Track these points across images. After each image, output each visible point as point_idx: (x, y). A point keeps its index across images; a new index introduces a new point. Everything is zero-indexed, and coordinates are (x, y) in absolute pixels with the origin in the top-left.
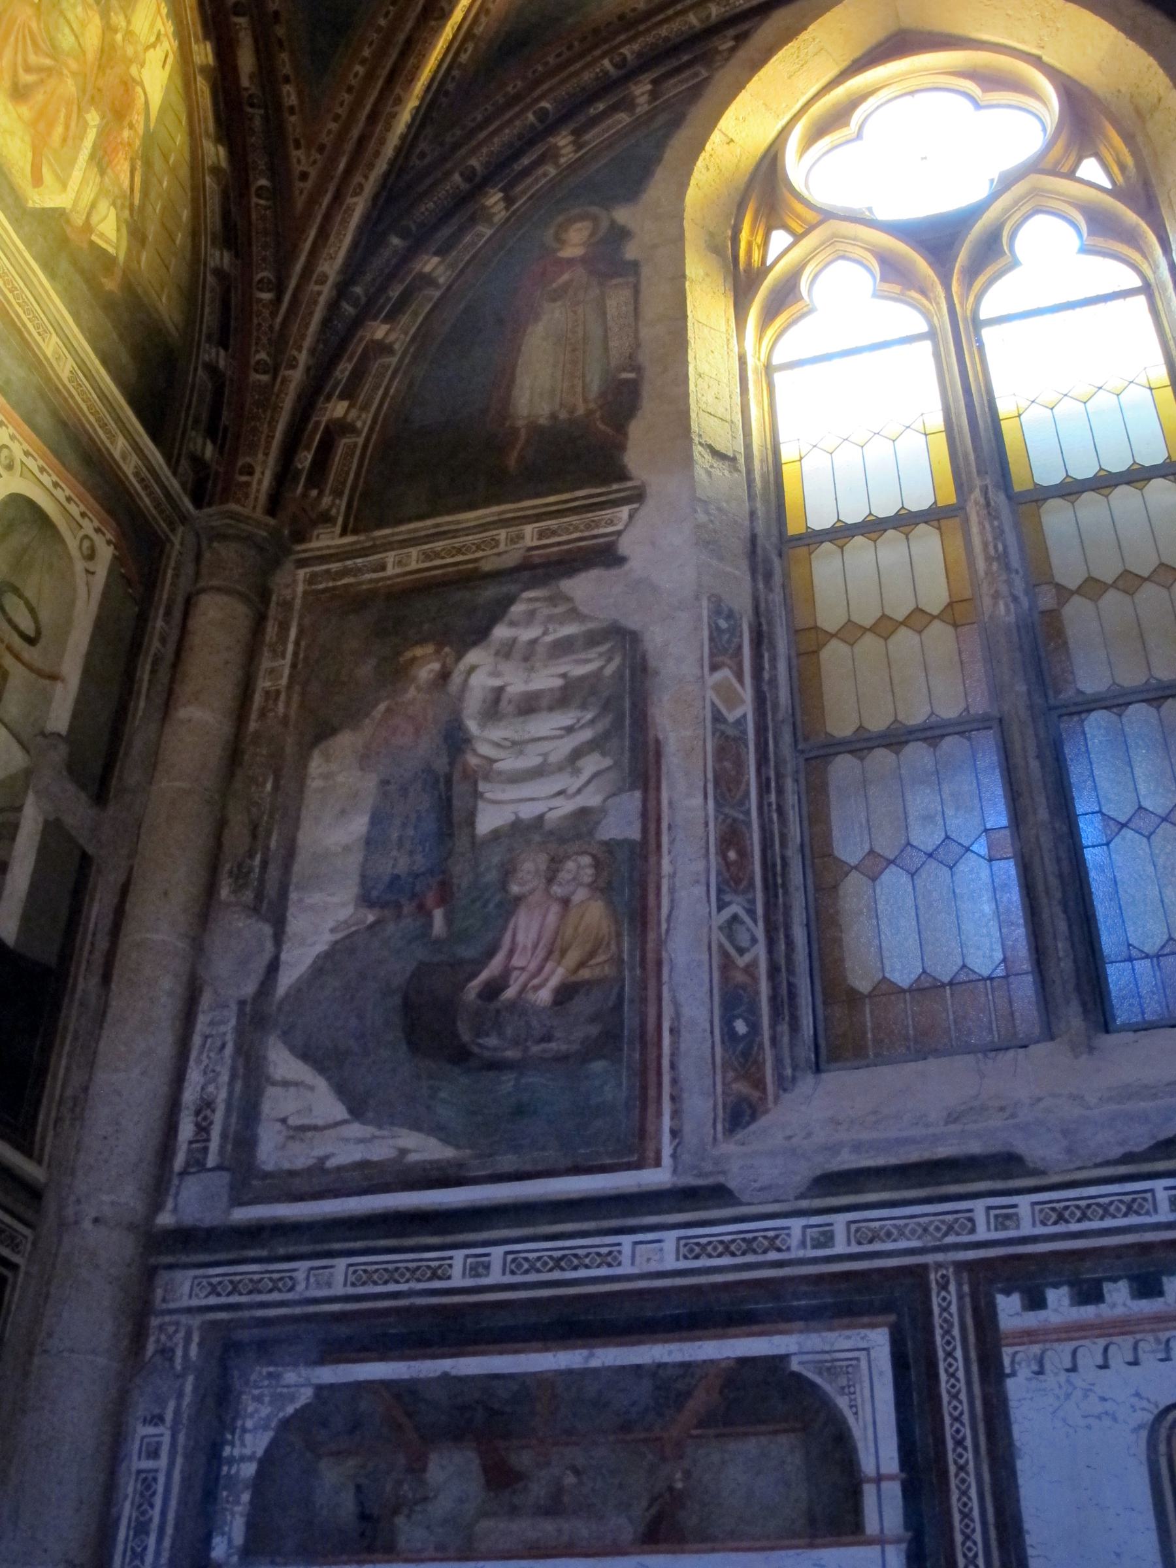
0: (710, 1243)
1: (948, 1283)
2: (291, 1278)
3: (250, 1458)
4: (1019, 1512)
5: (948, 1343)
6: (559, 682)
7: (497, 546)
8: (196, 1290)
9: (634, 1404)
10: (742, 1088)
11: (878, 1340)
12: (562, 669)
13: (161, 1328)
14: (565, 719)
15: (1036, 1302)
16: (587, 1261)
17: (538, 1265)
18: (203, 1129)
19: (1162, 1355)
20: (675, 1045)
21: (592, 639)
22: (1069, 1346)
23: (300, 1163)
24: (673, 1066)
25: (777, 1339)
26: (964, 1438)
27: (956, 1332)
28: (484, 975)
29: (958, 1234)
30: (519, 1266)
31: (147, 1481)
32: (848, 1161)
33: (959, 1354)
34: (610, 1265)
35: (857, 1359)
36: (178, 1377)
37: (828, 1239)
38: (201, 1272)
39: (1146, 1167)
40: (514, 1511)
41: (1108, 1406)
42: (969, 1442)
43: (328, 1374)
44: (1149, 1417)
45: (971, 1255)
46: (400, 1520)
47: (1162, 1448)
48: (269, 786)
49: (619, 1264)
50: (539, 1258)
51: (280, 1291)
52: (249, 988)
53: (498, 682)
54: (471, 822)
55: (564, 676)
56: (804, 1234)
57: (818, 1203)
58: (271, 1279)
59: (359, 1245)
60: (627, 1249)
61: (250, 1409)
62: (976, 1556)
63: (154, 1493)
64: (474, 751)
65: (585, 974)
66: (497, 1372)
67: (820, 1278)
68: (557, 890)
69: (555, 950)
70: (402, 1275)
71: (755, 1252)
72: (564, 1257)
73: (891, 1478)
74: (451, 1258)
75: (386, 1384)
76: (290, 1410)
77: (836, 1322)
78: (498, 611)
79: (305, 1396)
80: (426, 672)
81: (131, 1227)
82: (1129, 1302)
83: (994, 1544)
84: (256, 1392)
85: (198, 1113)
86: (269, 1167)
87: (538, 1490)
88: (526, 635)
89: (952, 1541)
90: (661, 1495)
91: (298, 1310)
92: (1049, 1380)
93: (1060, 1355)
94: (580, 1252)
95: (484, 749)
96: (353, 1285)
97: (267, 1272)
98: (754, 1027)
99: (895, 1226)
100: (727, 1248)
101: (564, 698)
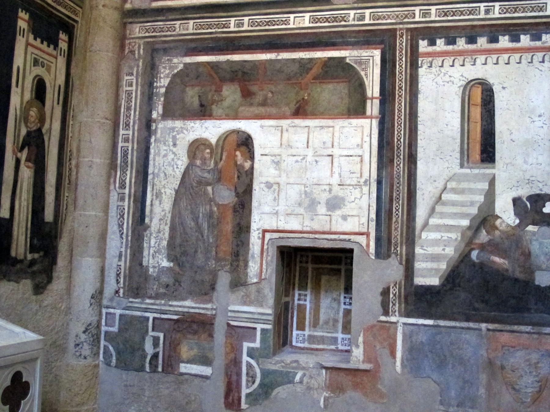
0: (321, 18)
1: (403, 35)
2: (174, 27)
4: (417, 111)
5: (401, 55)
8: (141, 31)
9: (292, 71)
11: (377, 54)
13: (130, 44)
15: (432, 43)
16: (278, 23)
17: (261, 24)
19: (472, 63)
22: (441, 59)
25: (342, 52)
26: (402, 87)
27: (404, 52)
29: (409, 18)
30: (254, 24)
31: (129, 94)
33: (404, 59)
34: (286, 24)
35: (369, 59)
36: (136, 60)
37: (362, 18)
38: (142, 25)
40: (251, 105)
41: (452, 79)
42: (403, 88)
43: (188, 60)
44: (464, 83)
45: (412, 26)
46: (214, 107)
47: (467, 93)
49: (289, 24)
50: (261, 21)
51: (170, 31)
56: (355, 16)
57: (360, 5)
58: (167, 27)
59: (198, 15)
60: (292, 19)
61: (162, 71)
62: (401, 123)
63: (132, 98)
66: (246, 59)
67: (359, 31)
70: (213, 26)
71: (337, 22)
72: (270, 21)
73: (376, 98)
74: (230, 21)
75: (208, 63)
76: (176, 71)
77: (363, 47)
79: (181, 66)
81: (116, 8)
82: (464, 45)
83: (407, 120)
84: (164, 65)
87: (259, 98)
89: (394, 119)
90: (300, 101)
91: (177, 38)
92: (433, 70)
93: (438, 61)
94: (276, 20)
96: (196, 29)
97: (165, 25)
99: (387, 15)
100: (327, 20)
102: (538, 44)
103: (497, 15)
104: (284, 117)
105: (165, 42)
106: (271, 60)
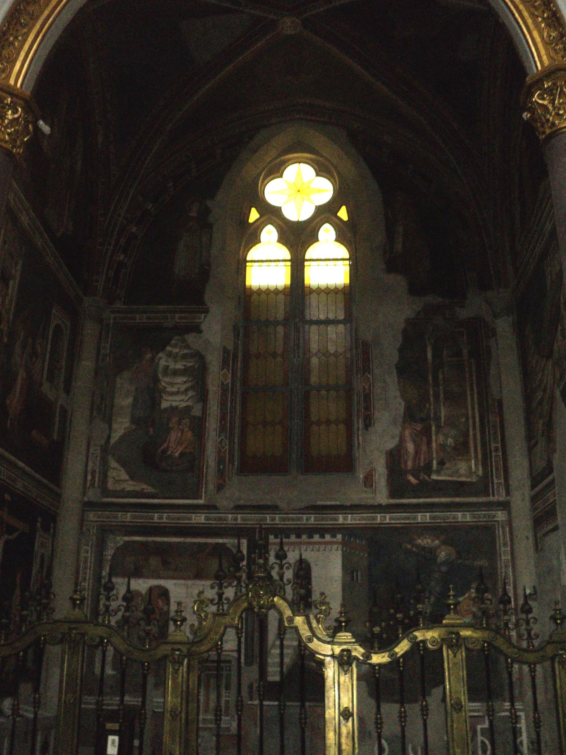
3: (110, 555)
6: (183, 367)
7: (168, 319)
10: (221, 482)
12: (185, 363)
14: (185, 379)
18: (93, 477)
20: (207, 472)
21: (192, 356)
23: (118, 489)
24: (206, 477)
28: (162, 448)
31: (86, 558)
32: (242, 502)
37: (236, 519)
39: (303, 512)
43: (126, 539)
48: (105, 384)
52: (103, 442)
53: (166, 364)
54: (160, 404)
55: (184, 366)
64: (161, 384)
65: (187, 450)
68: (180, 427)
69: (180, 443)
78: (167, 342)
79: (122, 543)
80: (149, 356)
85: (92, 473)
86: (111, 489)
88: (176, 350)
95: (163, 384)
98: (224, 467)
101: (185, 372)
102: (335, 540)
103: (313, 522)
104: (189, 578)
105: (111, 525)
106: (179, 543)
